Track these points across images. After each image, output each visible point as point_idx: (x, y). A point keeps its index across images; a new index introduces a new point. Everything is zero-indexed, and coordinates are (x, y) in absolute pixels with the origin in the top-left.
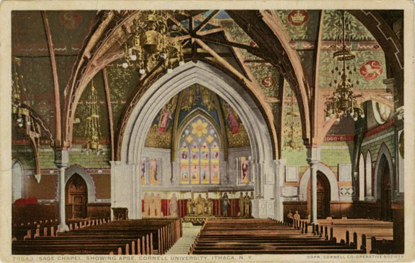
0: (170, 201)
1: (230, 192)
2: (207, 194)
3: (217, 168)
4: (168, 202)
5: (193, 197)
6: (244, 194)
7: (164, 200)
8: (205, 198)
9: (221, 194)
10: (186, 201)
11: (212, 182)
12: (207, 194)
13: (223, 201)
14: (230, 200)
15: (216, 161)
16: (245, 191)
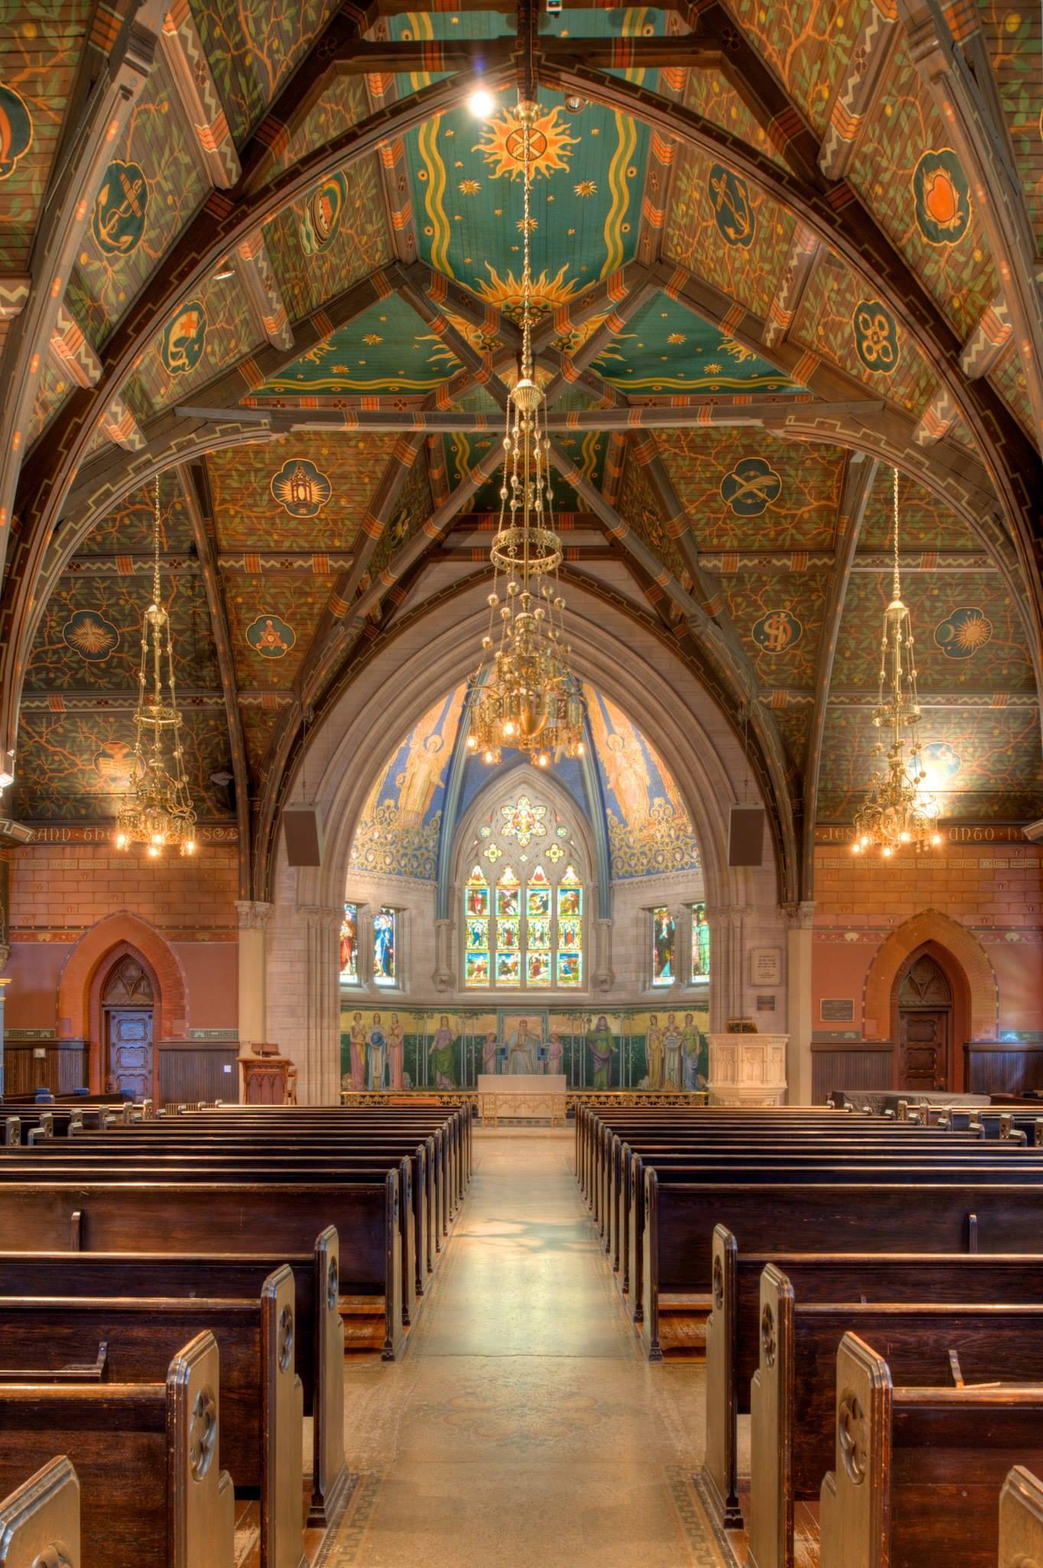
0: (431, 1038)
1: (615, 1013)
2: (544, 1021)
3: (575, 947)
4: (425, 1043)
5: (501, 1030)
6: (663, 1018)
7: (414, 1036)
8: (539, 1031)
9: (589, 1021)
10: (482, 1039)
11: (560, 984)
12: (544, 1021)
13: (594, 1042)
14: (616, 1039)
15: (571, 923)
16: (664, 1009)
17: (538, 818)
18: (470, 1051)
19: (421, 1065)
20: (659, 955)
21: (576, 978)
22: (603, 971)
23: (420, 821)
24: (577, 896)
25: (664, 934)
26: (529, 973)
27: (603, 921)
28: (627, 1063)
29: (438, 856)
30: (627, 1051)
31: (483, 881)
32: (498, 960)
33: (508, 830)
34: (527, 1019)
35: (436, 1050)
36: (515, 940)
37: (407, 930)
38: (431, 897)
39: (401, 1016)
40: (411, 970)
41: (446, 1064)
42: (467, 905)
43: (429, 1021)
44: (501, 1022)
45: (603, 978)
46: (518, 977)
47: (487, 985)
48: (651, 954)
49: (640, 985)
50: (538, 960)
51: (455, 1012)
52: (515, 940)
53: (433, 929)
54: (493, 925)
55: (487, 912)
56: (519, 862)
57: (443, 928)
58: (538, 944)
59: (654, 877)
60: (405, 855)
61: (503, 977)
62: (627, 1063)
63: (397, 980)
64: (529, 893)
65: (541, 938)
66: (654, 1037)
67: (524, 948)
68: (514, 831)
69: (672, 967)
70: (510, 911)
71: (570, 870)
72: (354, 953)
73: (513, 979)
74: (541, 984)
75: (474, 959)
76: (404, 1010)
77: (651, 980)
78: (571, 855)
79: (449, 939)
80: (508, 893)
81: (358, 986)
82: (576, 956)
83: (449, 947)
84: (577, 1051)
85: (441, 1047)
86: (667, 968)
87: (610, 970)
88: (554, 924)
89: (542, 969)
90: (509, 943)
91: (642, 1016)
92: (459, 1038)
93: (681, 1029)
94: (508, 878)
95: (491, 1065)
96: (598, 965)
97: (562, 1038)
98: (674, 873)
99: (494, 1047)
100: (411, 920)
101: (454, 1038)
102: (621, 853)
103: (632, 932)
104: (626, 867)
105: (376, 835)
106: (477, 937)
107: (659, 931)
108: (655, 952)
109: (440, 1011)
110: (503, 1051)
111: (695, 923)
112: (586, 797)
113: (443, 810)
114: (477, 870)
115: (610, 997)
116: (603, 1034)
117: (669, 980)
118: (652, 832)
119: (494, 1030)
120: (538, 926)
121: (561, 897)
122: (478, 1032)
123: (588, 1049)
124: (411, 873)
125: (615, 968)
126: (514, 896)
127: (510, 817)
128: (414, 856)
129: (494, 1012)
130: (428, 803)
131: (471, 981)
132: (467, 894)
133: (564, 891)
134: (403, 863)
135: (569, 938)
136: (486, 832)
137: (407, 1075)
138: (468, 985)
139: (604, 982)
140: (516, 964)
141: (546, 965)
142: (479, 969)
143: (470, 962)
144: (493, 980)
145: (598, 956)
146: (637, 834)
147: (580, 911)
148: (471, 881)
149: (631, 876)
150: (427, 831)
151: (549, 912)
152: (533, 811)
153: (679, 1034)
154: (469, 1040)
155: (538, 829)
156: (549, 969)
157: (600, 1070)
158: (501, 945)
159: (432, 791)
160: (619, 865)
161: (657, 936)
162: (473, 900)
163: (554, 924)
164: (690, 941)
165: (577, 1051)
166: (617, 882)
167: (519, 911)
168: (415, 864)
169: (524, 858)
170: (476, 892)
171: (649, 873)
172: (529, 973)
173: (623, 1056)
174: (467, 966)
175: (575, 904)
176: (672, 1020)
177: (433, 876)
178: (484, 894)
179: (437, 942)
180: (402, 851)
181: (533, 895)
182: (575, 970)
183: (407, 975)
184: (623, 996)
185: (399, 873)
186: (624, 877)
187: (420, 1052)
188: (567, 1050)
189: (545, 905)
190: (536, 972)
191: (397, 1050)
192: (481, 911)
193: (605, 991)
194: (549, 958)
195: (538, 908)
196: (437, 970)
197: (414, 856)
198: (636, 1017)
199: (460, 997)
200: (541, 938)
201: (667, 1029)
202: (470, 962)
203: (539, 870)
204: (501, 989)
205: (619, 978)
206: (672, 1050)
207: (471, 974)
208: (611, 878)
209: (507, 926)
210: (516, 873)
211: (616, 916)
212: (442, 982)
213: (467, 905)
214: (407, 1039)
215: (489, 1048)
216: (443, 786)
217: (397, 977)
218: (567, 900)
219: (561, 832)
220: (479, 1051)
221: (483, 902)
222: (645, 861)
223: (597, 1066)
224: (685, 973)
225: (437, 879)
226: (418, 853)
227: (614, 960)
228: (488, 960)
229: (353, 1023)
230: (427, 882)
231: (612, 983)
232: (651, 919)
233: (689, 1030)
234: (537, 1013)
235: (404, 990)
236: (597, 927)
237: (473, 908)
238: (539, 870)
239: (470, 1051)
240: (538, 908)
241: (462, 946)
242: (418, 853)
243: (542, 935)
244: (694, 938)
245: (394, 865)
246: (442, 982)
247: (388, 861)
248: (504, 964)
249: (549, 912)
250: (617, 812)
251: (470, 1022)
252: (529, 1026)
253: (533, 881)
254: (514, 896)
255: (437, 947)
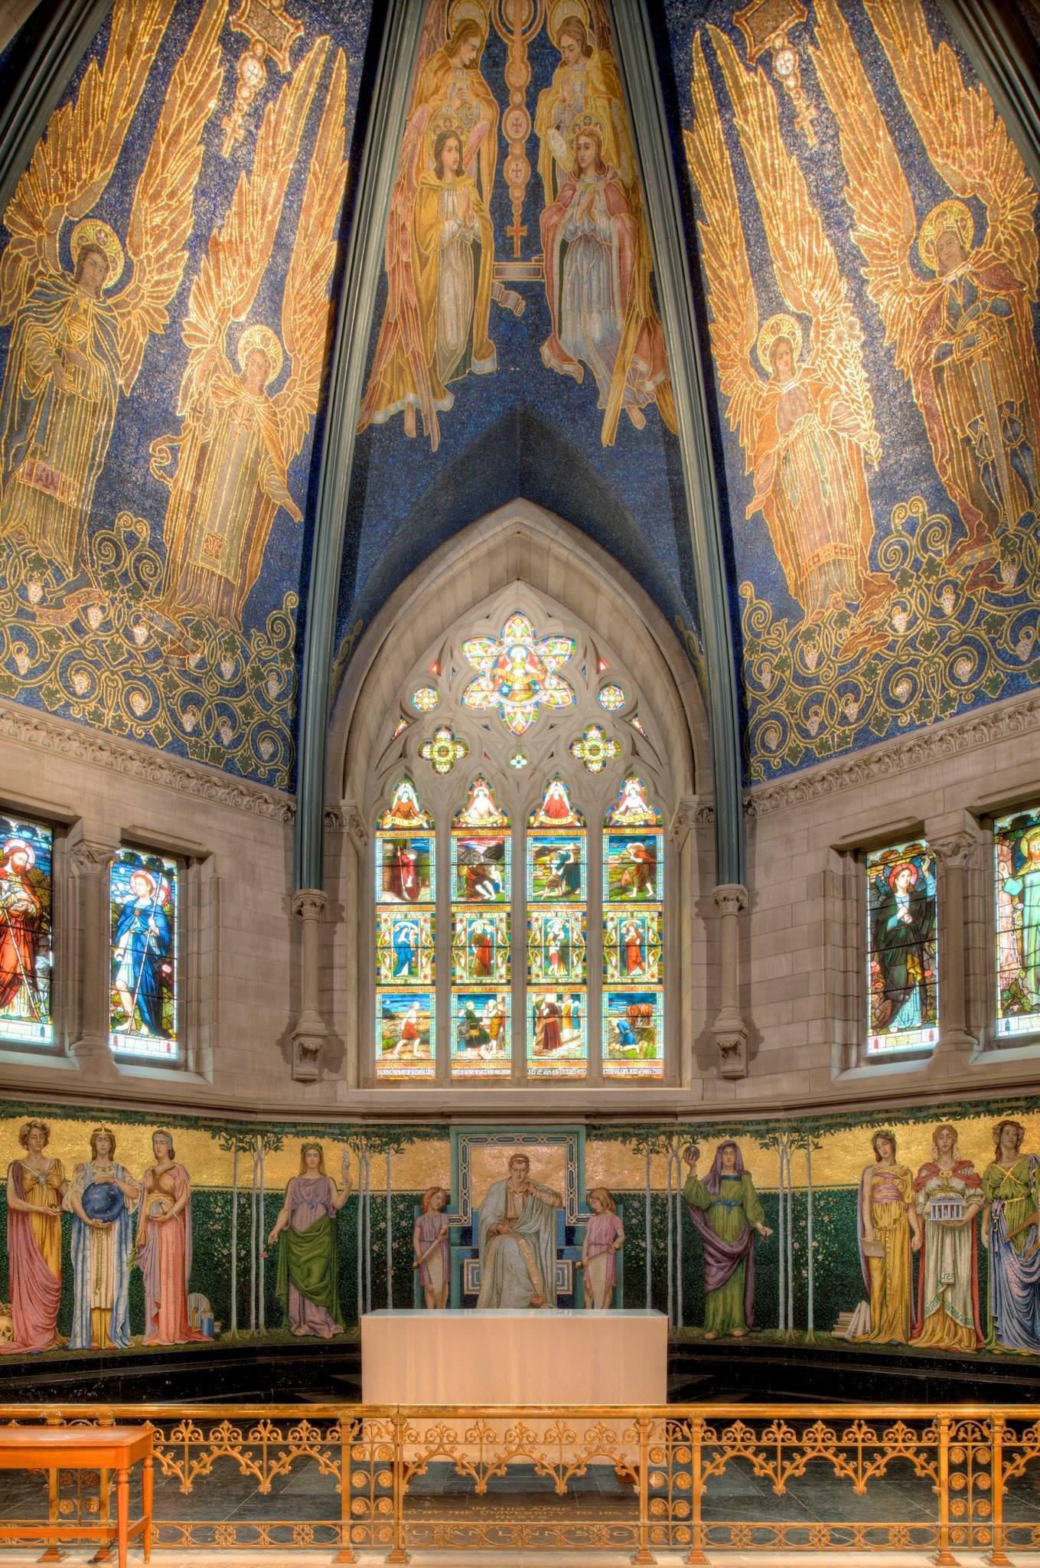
0: (275, 1200)
1: (765, 1133)
2: (574, 1157)
3: (647, 974)
4: (258, 1213)
5: (462, 1181)
7: (225, 1196)
8: (560, 1184)
9: (693, 1155)
10: (411, 1203)
11: (610, 1068)
12: (574, 1157)
13: (705, 1211)
14: (768, 1200)
16: (918, 1114)
17: (552, 665)
18: (379, 1236)
19: (245, 1272)
20: (886, 971)
21: (648, 1055)
22: (729, 1021)
23: (237, 604)
24: (651, 853)
25: (903, 913)
26: (532, 1043)
27: (730, 888)
28: (799, 1262)
29: (295, 726)
30: (799, 1233)
31: (419, 820)
32: (457, 1010)
33: (480, 697)
34: (530, 1150)
35: (288, 1231)
36: (498, 959)
37: (207, 912)
38: (278, 835)
39: (184, 1140)
40: (216, 1018)
41: (317, 1269)
42: (380, 877)
43: (270, 1158)
44: (461, 1162)
45: (730, 1040)
46: (507, 1052)
47: (430, 1072)
48: (860, 972)
49: (836, 1051)
50: (554, 1011)
51: (341, 1133)
52: (500, 964)
53: (282, 917)
54: (443, 926)
55: (427, 894)
56: (505, 772)
57: (310, 912)
58: (557, 971)
59: (879, 749)
60: (192, 700)
61: (470, 1053)
62: (799, 1262)
63: (184, 1047)
64: (532, 846)
65: (563, 957)
66: (885, 1193)
67: (520, 980)
68: (495, 698)
69: (926, 1001)
70: (485, 890)
71: (632, 787)
72: (43, 962)
73: (492, 1059)
74: (561, 1070)
75: (395, 1008)
76: (193, 1123)
77: (862, 1042)
78: (635, 753)
79: (326, 948)
80: (481, 849)
81: (58, 1051)
82: (650, 998)
83: (326, 968)
84: (660, 1234)
85: (302, 1224)
86: (911, 1008)
87: (747, 1021)
88: (595, 923)
89: (566, 1033)
90: (485, 968)
91: (844, 1137)
92: (352, 1201)
93: (980, 1168)
94: (481, 810)
95: (435, 1274)
96: (714, 1009)
97: (620, 1201)
98: (949, 721)
99: (443, 1222)
100: (217, 882)
101: (339, 1201)
102: (780, 705)
103: (811, 913)
104: (794, 739)
105: (95, 618)
106: (406, 955)
107: (887, 904)
108: (872, 966)
109: (299, 1130)
110: (467, 1235)
111: (1004, 870)
112: (685, 552)
113: (304, 590)
114: (405, 793)
115: (746, 1093)
116: (730, 1190)
117: (926, 1038)
118: (879, 615)
119: (445, 1182)
120: (556, 927)
121: (611, 856)
122: (404, 1185)
123: (690, 1230)
124: (216, 756)
125: (760, 1015)
126: (497, 854)
127: (486, 665)
128: (223, 709)
129: (443, 1132)
130: (256, 559)
131: (389, 1064)
132: (380, 852)
133: (622, 840)
134: (188, 722)
135: (630, 953)
136: (424, 700)
137: (201, 1303)
138: (382, 1072)
139: (728, 1051)
140: (501, 1018)
141: (574, 1019)
142: (410, 1034)
143: (389, 1016)
144: (444, 1060)
145: (714, 989)
146: (833, 637)
147: (658, 889)
148: (389, 821)
149: (809, 759)
150: (258, 645)
151: (582, 893)
152: (542, 649)
153: (975, 1181)
154: (378, 1205)
155: (556, 694)
156: (583, 1032)
157: (724, 1282)
158: (463, 971)
159: (268, 523)
160: (773, 739)
161: (879, 923)
162: (394, 865)
163: (595, 923)
164: (989, 919)
165: (660, 1234)
166: (764, 786)
167: (507, 893)
168: (227, 736)
169: (519, 763)
170: (401, 845)
171: (864, 738)
172: (532, 1043)
173: (786, 1246)
174: (381, 1027)
175: (646, 871)
176: (945, 1142)
177: (283, 777)
178: (422, 852)
179: (295, 954)
180: (184, 687)
181: (541, 853)
182: (647, 1035)
183: (206, 1032)
184: (788, 1087)
185: (177, 748)
186: (786, 769)
187: (243, 1238)
188: (633, 1233)
189: (571, 874)
190: (551, 1039)
191: (169, 1232)
192: (414, 892)
193: (733, 1078)
194: (582, 1006)
195: (554, 884)
196: (293, 1025)
197: (223, 709)
198: (826, 1140)
199: (347, 1094)
200: (563, 957)
201: (932, 1169)
202: (389, 1016)
203: (557, 791)
204: (463, 1081)
205: (772, 1040)
206: (944, 1229)
207: (389, 1047)
208: (747, 782)
209: (478, 927)
210: (501, 801)
211: (761, 879)
212: (306, 1053)
213: (380, 877)
214: (202, 1203)
215: (430, 1225)
216: (299, 518)
217: (182, 1038)
218: (625, 863)
219: (612, 699)
220: (405, 1236)
221: (419, 867)
222: (852, 710)
223: (714, 1274)
224: (978, 1008)
225: (292, 788)
226: (236, 705)
227: (756, 993)
228: (432, 1009)
229: (21, 1153)
230: (266, 791)
231: (752, 1055)
232: (860, 879)
233: (1008, 1169)
234: (554, 1139)
235: (200, 1073)
236: (709, 910)
237: (394, 886)
238: (557, 791)
239: (379, 1236)
240: (554, 884)
241: (366, 981)
242: (236, 705)
243: (565, 947)
244: (1003, 910)
245: (160, 721)
246: (306, 1053)
247: (140, 705)
248: (471, 1020)
249: (582, 893)
250: (771, 584)
251: (378, 1159)
252: (535, 1167)
253: (543, 818)
254: (497, 853)
255: (295, 966)
